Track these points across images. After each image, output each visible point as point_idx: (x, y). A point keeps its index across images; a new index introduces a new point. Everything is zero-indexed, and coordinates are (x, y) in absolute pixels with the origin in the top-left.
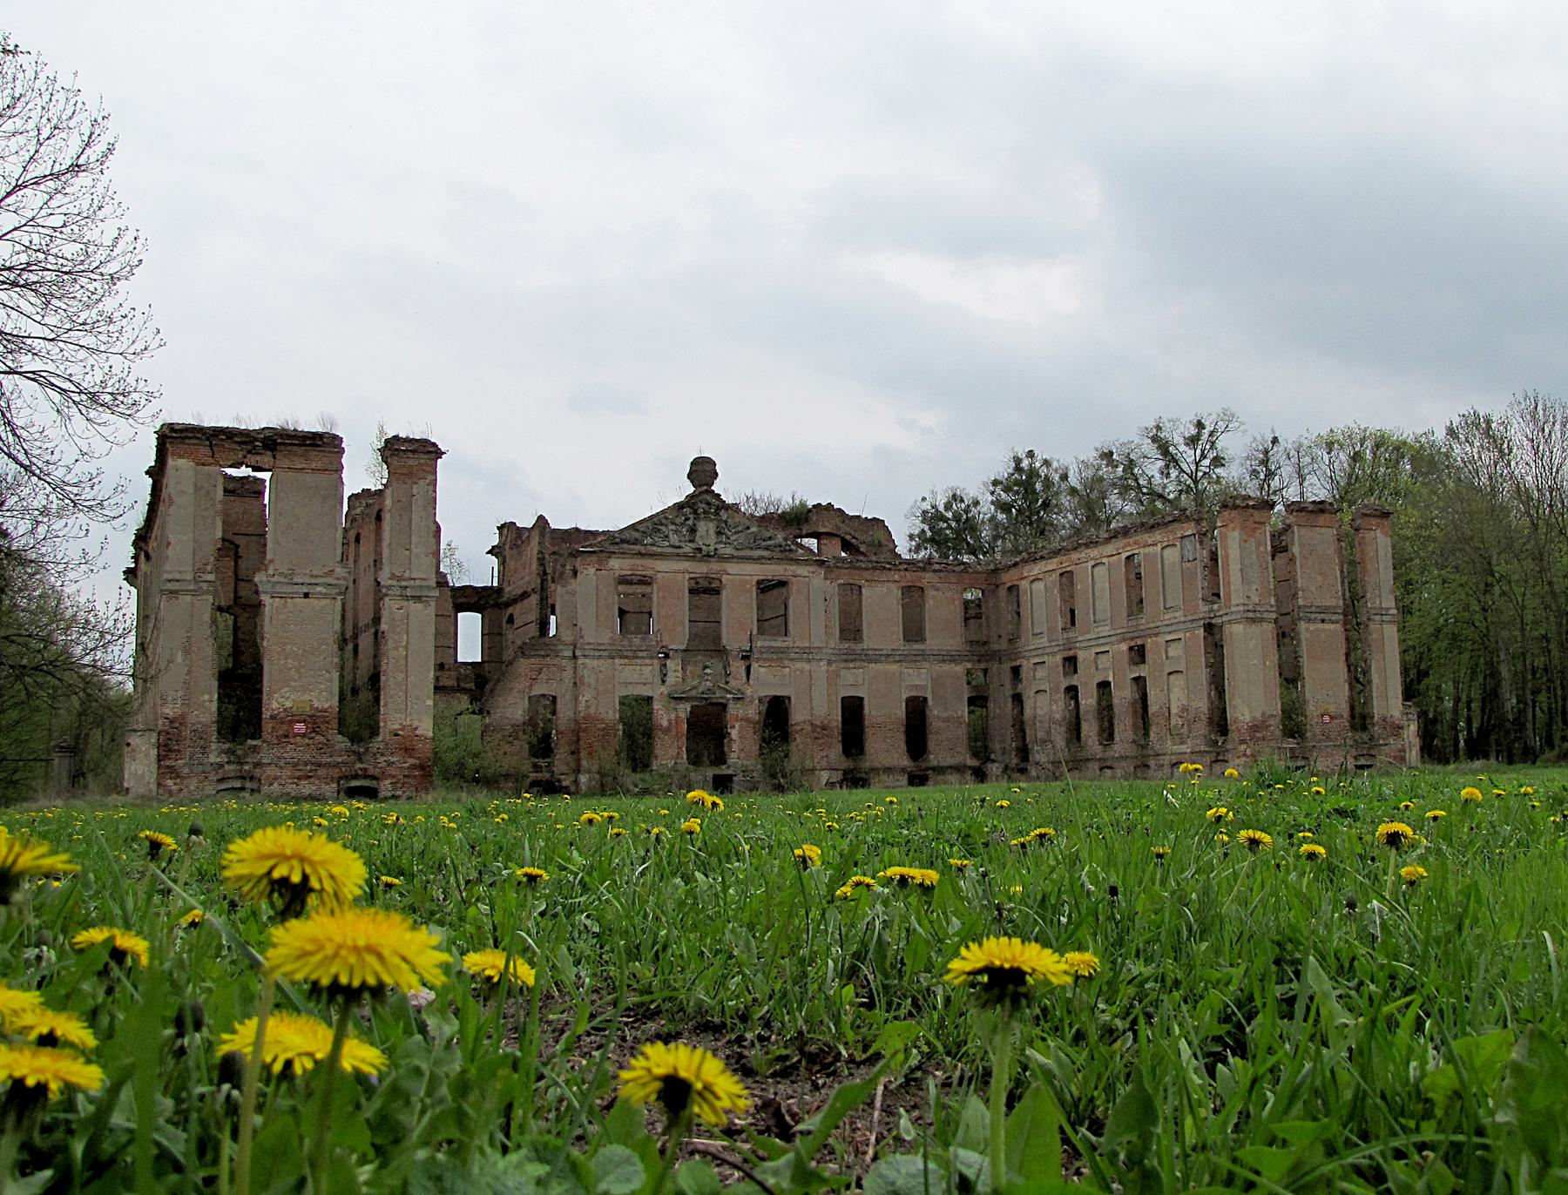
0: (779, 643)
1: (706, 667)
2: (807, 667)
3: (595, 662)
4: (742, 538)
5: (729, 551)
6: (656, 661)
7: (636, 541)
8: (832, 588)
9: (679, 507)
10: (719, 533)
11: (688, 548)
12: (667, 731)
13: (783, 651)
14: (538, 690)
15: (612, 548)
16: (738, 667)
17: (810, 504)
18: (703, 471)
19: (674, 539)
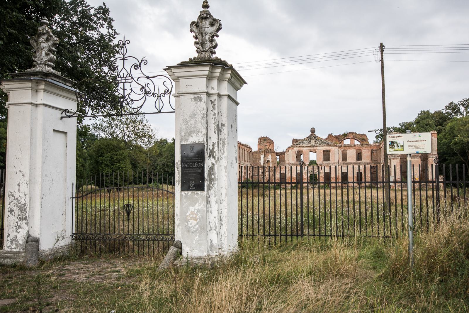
0: (328, 162)
4: (320, 142)
5: (318, 145)
7: (299, 144)
8: (340, 151)
10: (315, 142)
11: (309, 145)
18: (313, 130)
19: (307, 143)
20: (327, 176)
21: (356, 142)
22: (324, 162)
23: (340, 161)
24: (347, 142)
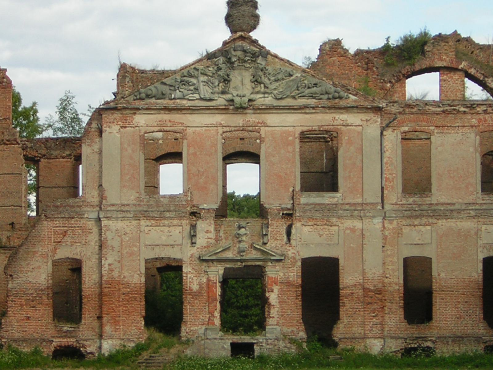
0: (327, 198)
1: (240, 227)
2: (358, 224)
3: (120, 225)
4: (280, 87)
5: (269, 100)
6: (185, 222)
7: (163, 96)
8: (392, 137)
9: (210, 56)
10: (256, 81)
11: (221, 101)
12: (196, 295)
13: (332, 209)
14: (64, 253)
15: (138, 104)
16: (277, 227)
17: (433, 33)
19: (205, 91)
20: (321, 283)
21: (474, 91)
22: (306, 199)
23: (394, 196)
24: (424, 87)
